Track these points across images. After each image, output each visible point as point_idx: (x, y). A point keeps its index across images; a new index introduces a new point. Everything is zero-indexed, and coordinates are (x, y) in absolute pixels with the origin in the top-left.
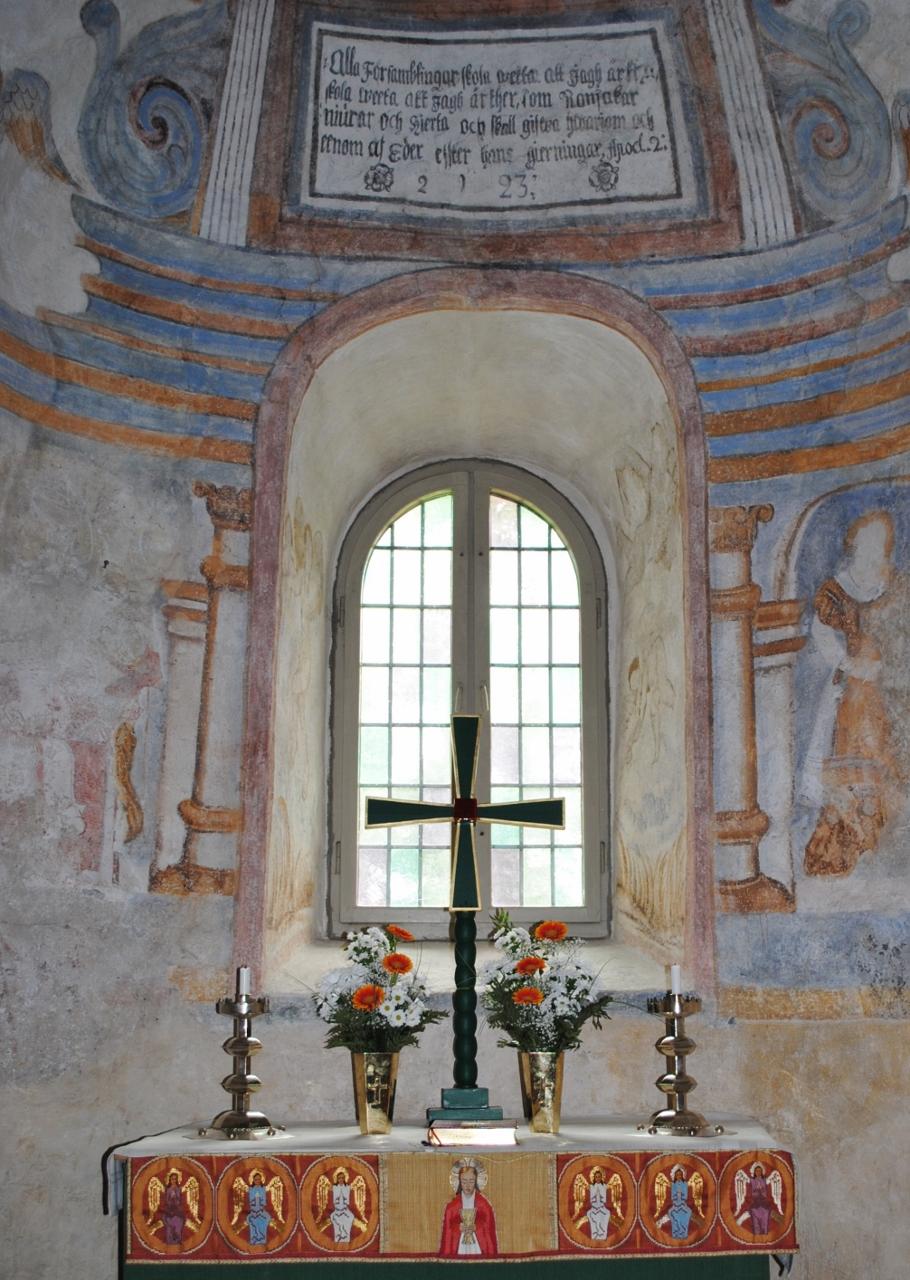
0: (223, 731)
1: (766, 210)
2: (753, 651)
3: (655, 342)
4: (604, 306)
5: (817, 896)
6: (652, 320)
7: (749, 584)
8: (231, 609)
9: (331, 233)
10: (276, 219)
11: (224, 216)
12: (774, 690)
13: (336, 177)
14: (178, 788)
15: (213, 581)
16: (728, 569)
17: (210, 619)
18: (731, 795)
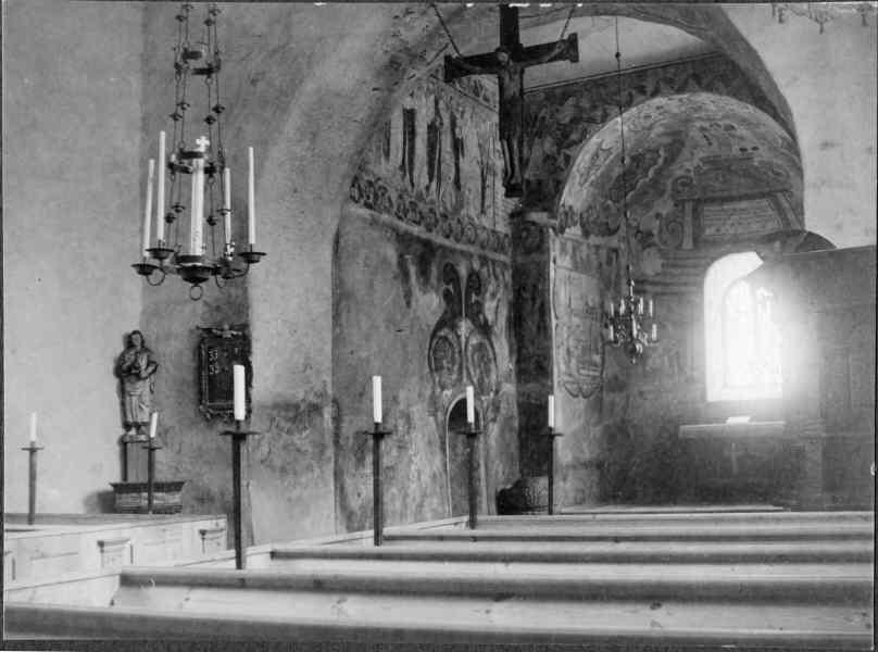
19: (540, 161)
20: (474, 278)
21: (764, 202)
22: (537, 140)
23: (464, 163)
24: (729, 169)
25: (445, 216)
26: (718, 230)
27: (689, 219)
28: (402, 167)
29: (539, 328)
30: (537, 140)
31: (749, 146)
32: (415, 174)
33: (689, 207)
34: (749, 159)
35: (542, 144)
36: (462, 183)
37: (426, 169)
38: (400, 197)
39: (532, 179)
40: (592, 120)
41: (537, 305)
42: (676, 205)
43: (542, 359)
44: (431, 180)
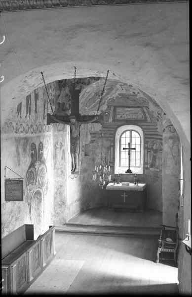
0: (112, 157)
1: (149, 120)
2: (148, 152)
3: (141, 128)
4: (138, 125)
5: (151, 169)
6: (141, 127)
7: (147, 147)
8: (112, 149)
9: (118, 120)
10: (114, 120)
11: (111, 120)
12: (149, 154)
13: (118, 117)
14: (109, 161)
15: (111, 146)
16: (146, 145)
17: (110, 149)
18: (146, 162)
19: (64, 95)
20: (41, 144)
21: (139, 109)
22: (63, 89)
23: (38, 104)
24: (128, 98)
25: (32, 126)
26: (121, 116)
27: (111, 112)
28: (18, 112)
29: (62, 159)
30: (63, 89)
31: (136, 92)
32: (22, 113)
33: (112, 109)
34: (136, 96)
35: (65, 90)
36: (37, 110)
37: (25, 108)
38: (17, 124)
39: (60, 102)
40: (85, 84)
41: (62, 150)
42: (108, 107)
43: (63, 169)
44: (27, 113)
